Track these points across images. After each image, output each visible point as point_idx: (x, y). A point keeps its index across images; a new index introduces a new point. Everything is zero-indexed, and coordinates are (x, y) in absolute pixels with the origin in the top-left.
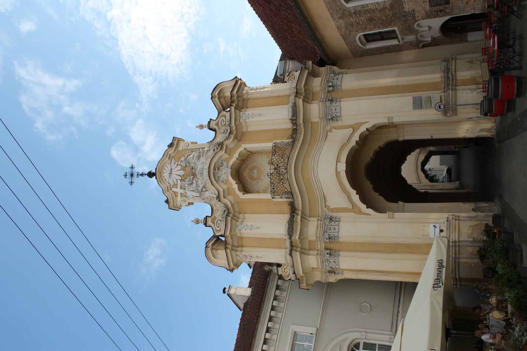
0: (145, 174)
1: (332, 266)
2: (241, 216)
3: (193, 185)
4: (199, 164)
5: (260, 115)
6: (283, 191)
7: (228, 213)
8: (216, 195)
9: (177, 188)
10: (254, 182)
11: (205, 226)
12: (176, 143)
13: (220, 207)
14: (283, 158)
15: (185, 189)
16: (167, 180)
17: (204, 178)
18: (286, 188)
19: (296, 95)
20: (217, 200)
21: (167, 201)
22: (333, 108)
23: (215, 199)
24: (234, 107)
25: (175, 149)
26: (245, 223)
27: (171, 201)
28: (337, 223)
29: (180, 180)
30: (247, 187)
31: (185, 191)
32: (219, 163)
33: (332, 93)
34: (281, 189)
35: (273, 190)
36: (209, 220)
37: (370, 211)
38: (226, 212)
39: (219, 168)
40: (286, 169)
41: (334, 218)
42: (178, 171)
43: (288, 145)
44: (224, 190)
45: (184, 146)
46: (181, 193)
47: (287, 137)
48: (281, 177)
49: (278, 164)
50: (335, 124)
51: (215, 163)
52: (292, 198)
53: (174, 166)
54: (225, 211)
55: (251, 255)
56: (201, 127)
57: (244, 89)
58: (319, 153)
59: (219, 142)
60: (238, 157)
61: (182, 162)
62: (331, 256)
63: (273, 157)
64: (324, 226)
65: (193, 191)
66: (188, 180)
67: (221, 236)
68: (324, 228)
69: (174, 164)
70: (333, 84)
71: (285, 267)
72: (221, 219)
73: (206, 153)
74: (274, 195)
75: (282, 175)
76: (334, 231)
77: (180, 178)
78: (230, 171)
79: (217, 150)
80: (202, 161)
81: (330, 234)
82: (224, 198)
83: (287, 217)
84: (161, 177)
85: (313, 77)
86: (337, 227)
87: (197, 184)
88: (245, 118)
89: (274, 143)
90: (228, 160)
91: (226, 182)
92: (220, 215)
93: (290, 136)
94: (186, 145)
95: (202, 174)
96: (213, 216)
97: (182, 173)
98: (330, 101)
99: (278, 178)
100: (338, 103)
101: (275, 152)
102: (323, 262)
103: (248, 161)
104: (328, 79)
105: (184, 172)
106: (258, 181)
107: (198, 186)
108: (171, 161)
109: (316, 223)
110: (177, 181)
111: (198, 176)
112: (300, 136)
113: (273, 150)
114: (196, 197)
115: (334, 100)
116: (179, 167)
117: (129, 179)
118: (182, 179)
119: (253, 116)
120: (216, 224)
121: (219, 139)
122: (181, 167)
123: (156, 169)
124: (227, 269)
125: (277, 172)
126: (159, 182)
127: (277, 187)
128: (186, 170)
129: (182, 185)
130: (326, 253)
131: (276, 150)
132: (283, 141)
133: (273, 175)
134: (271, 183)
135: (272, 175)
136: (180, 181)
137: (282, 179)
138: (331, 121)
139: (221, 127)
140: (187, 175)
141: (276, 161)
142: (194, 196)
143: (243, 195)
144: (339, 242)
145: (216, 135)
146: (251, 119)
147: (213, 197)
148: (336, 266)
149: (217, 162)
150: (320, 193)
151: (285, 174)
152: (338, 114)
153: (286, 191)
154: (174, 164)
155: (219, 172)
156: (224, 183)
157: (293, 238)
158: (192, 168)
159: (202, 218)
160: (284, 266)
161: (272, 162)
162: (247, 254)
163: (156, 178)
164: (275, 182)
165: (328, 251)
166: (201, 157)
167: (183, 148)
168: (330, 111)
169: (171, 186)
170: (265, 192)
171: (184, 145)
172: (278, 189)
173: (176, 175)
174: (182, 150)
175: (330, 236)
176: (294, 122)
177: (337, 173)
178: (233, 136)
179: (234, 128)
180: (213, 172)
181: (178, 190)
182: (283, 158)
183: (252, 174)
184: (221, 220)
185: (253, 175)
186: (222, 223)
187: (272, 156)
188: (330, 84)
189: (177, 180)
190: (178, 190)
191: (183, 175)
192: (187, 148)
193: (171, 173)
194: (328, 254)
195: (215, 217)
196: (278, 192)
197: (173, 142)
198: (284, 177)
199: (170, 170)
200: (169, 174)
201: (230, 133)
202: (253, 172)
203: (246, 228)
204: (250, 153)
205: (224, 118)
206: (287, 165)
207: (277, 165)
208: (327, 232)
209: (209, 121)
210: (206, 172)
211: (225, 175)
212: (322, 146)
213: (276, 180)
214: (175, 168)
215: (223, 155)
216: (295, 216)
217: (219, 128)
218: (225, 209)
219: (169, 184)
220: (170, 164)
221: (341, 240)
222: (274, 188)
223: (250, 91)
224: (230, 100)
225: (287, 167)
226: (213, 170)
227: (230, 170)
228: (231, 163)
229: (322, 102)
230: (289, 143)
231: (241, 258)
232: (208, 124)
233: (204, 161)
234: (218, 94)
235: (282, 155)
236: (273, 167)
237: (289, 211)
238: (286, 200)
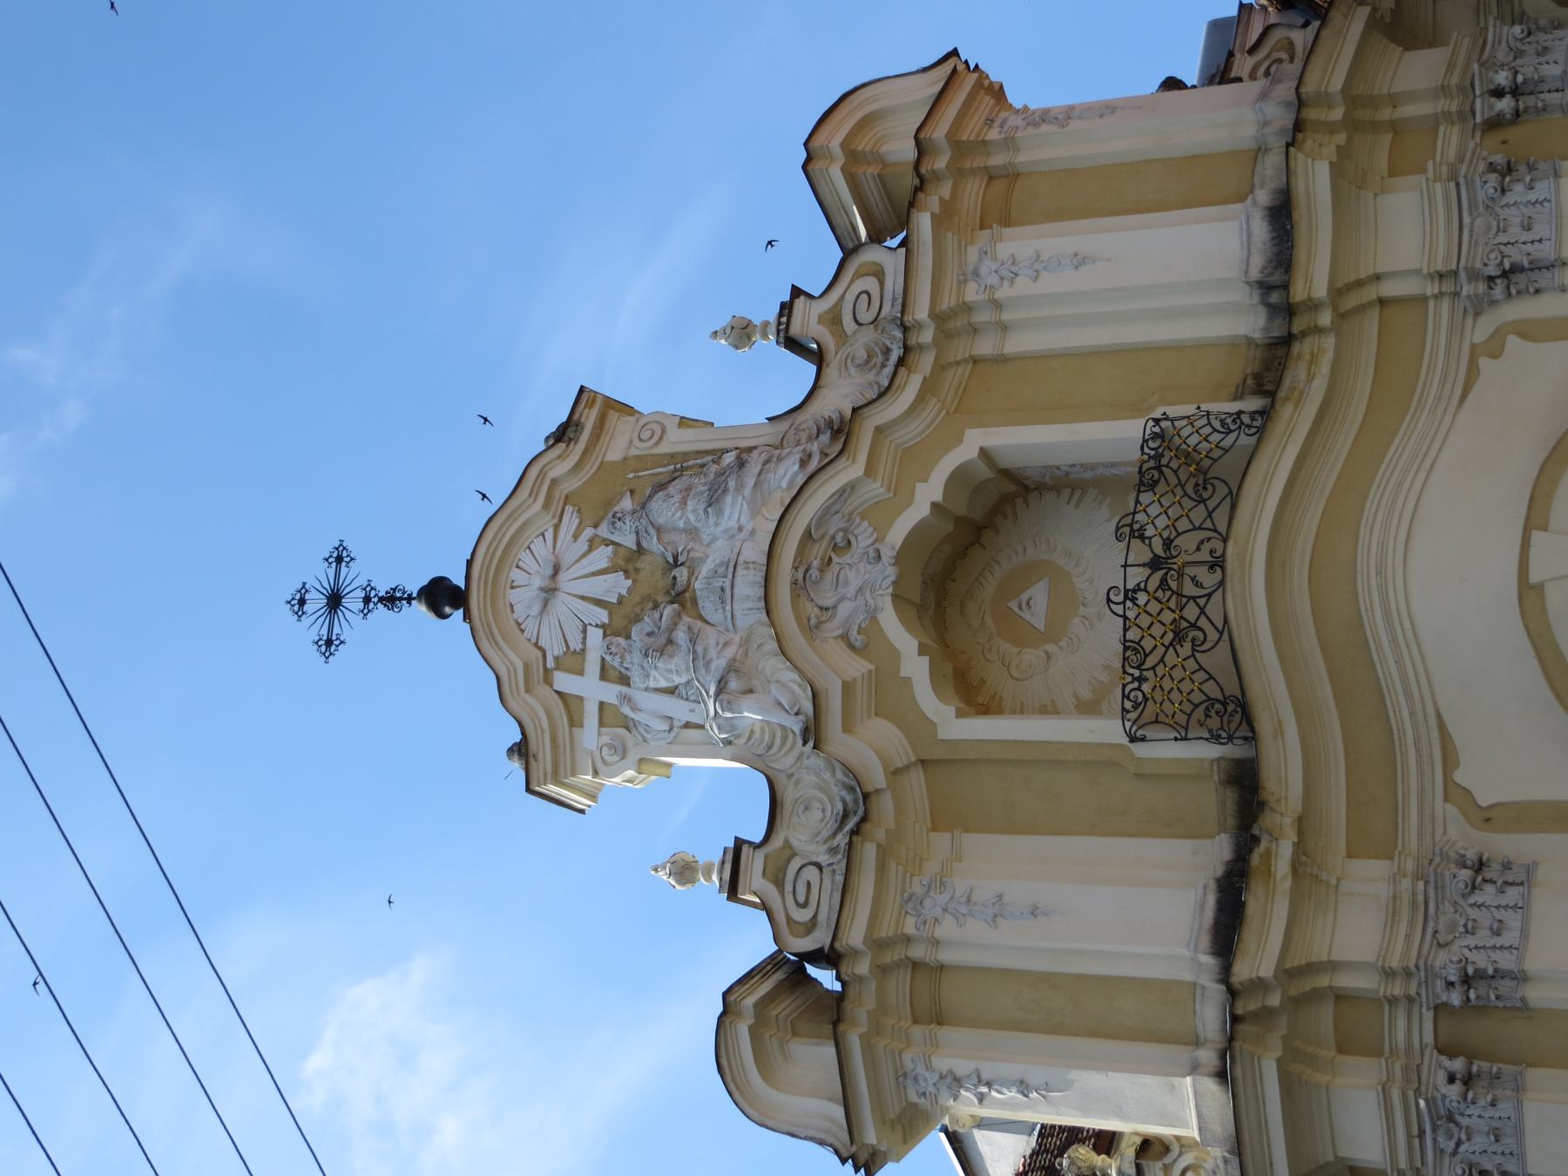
0: (410, 595)
1: (1475, 1159)
3: (671, 656)
4: (714, 539)
5: (1080, 261)
6: (1197, 697)
7: (864, 819)
8: (801, 717)
9: (581, 673)
10: (1031, 656)
11: (729, 898)
12: (590, 419)
13: (825, 792)
14: (1204, 501)
15: (625, 680)
16: (531, 627)
17: (738, 615)
18: (1211, 677)
19: (1294, 138)
20: (805, 743)
21: (521, 750)
22: (1514, 216)
23: (794, 744)
24: (933, 215)
25: (586, 452)
26: (960, 885)
27: (541, 746)
28: (1513, 895)
29: (603, 626)
30: (983, 682)
31: (624, 689)
32: (831, 532)
33: (1510, 133)
34: (1186, 686)
35: (1139, 689)
36: (754, 866)
38: (850, 825)
39: (830, 560)
40: (1217, 563)
41: (1495, 866)
42: (594, 574)
43: (1233, 427)
44: (848, 688)
45: (636, 442)
46: (602, 704)
47: (1233, 389)
48: (1186, 612)
49: (1174, 534)
51: (808, 535)
52: (1246, 739)
53: (571, 550)
54: (845, 816)
55: (985, 1076)
56: (741, 333)
57: (992, 121)
58: (1422, 475)
59: (835, 417)
60: (938, 496)
61: (619, 524)
62: (1470, 1095)
63: (1146, 498)
64: (1437, 908)
65: (671, 691)
66: (647, 624)
67: (818, 957)
68: (1437, 921)
69: (576, 537)
70: (1520, 79)
71: (1188, 1159)
72: (823, 859)
73: (759, 474)
74: (1141, 722)
75: (1194, 598)
76: (1498, 941)
77: (602, 616)
78: (893, 578)
79: (820, 461)
80: (733, 523)
81: (1472, 956)
82: (847, 728)
83: (1217, 851)
84: (493, 608)
85: (1399, 45)
86: (1513, 920)
87: (695, 652)
88: (993, 279)
89: (1157, 421)
90: (881, 514)
91: (866, 642)
92: (818, 834)
93: (1250, 381)
94: (646, 435)
95: (725, 596)
96: (777, 842)
97: (615, 586)
98: (1496, 175)
99: (1167, 617)
100: (1542, 189)
101: (1158, 468)
102: (1422, 1133)
103: (998, 532)
104: (1486, 54)
105: (629, 582)
106: (1050, 647)
107: (700, 663)
108: (556, 521)
109: (1383, 890)
110: (584, 631)
111: (707, 606)
112: (1310, 378)
113: (1146, 457)
114: (688, 725)
115: (1523, 168)
116: (602, 557)
117: (313, 626)
118: (610, 624)
119: (1038, 266)
120: (789, 887)
121: (838, 399)
122: (615, 553)
123: (469, 563)
124: (837, 1152)
125: (1164, 585)
126: (481, 634)
127: (1160, 670)
128: (637, 570)
129: (608, 658)
130: (1441, 1077)
131: (1162, 455)
132: (1204, 407)
133: (1142, 598)
134: (1126, 649)
135: (1133, 600)
136: (600, 631)
137: (1193, 626)
138: (1498, 291)
139: (855, 332)
140: (646, 598)
141: (1162, 522)
142: (676, 724)
143: (957, 717)
144: (1524, 1007)
145: (824, 381)
146: (1024, 286)
147: (783, 728)
148: (1498, 1159)
150: (1420, 715)
151: (1209, 595)
152: (1546, 252)
153: (1211, 689)
154: (576, 537)
155: (829, 576)
156: (851, 647)
157: (1242, 971)
158: (676, 558)
159: (711, 851)
160: (1181, 1154)
161: (1136, 527)
162: (962, 1067)
163: (467, 617)
164: (1148, 644)
165: (1458, 1065)
166: (729, 499)
167: (633, 452)
168: (1496, 234)
169: (550, 664)
170: (1088, 708)
171: (636, 434)
172: (1167, 684)
173: (583, 598)
174: (625, 459)
175: (1470, 970)
176: (1275, 297)
178: (912, 386)
179: (927, 336)
180: (795, 583)
181: (590, 688)
182: (1204, 501)
183: (1020, 607)
184: (819, 867)
185: (1026, 615)
186: (827, 883)
187: (1139, 492)
188: (1502, 78)
189: (585, 626)
190: (590, 688)
191: (621, 599)
192: (651, 447)
193: (549, 592)
194: (1451, 1079)
195: (787, 841)
196: (1167, 703)
197: (576, 417)
198: (1202, 612)
199: (550, 571)
200: (542, 589)
201: (901, 362)
202: (1024, 597)
203: (964, 910)
204: (1013, 488)
205: (871, 284)
206: (1225, 540)
207: (1168, 543)
208: (1455, 947)
209: (787, 298)
210: (748, 586)
211: (860, 602)
212: (1441, 435)
213: (1157, 630)
214: (577, 557)
215: (852, 487)
216: (1263, 845)
217: (842, 337)
218: (849, 798)
219: (540, 648)
220: (549, 535)
221: (1536, 995)
222: (1141, 680)
223: (1030, 130)
224: (910, 181)
225: (1223, 554)
226: (796, 569)
227: (892, 572)
229: (1449, 180)
230: (1246, 419)
231: (924, 1094)
232: (781, 315)
233: (743, 520)
234: (843, 145)
235: (1197, 484)
236: (1140, 553)
237: (1231, 822)
238: (1211, 751)
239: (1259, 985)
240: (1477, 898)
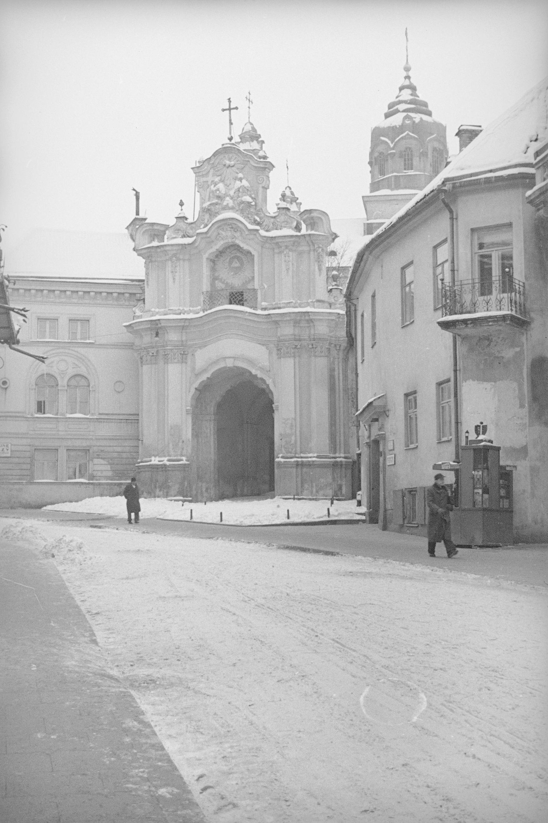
2: (187, 257)
5: (288, 270)
37: (193, 391)
50: (275, 351)
81: (170, 356)
86: (176, 361)
88: (285, 252)
149: (238, 227)
165: (155, 354)
177: (225, 358)
194: (153, 353)
202: (237, 262)
228: (237, 242)
239: (160, 324)
240: (179, 355)
